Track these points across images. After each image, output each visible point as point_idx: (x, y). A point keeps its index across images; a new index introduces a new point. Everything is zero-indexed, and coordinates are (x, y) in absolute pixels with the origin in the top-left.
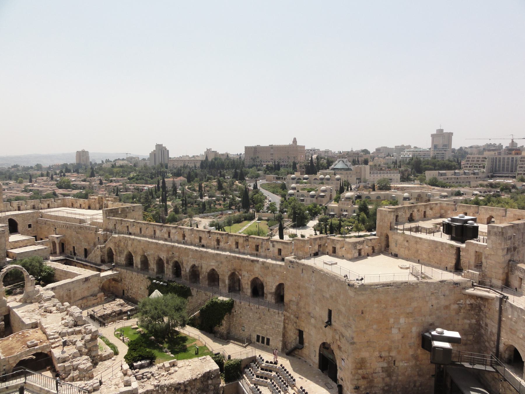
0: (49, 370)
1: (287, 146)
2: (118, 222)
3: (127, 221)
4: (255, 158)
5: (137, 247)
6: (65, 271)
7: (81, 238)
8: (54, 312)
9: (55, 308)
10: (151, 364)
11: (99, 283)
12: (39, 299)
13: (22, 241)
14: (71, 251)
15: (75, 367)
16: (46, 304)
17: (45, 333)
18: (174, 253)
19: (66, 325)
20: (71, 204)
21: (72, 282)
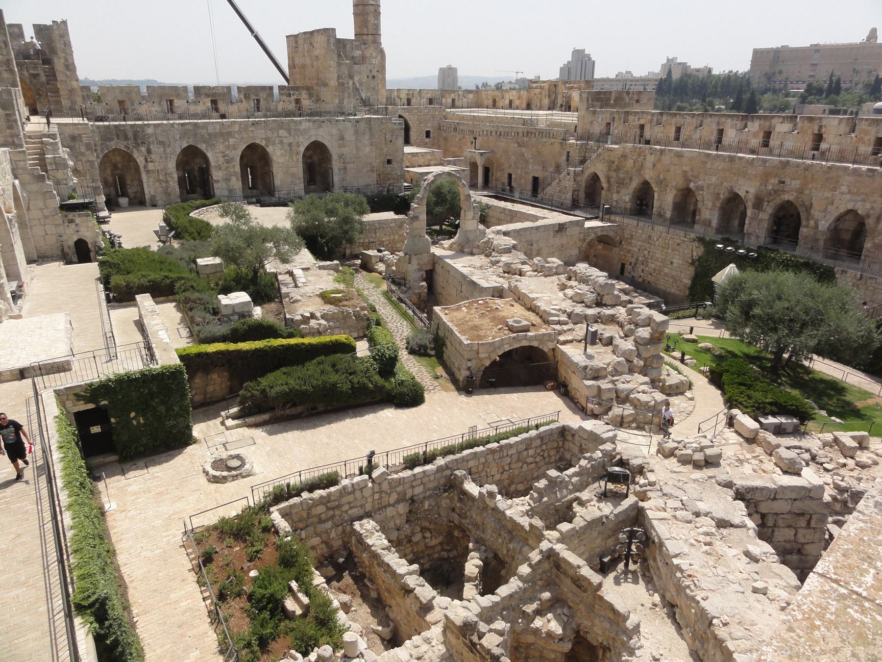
0: (552, 389)
1: (857, 44)
2: (616, 116)
3: (643, 112)
4: (774, 74)
5: (668, 171)
6: (510, 210)
7: (528, 155)
8: (528, 273)
9: (526, 268)
10: (796, 432)
11: (580, 240)
12: (488, 250)
13: (422, 154)
14: (503, 183)
15: (623, 395)
16: (505, 258)
17: (532, 309)
18: (788, 181)
19: (579, 300)
20: (491, 102)
21: (537, 228)
